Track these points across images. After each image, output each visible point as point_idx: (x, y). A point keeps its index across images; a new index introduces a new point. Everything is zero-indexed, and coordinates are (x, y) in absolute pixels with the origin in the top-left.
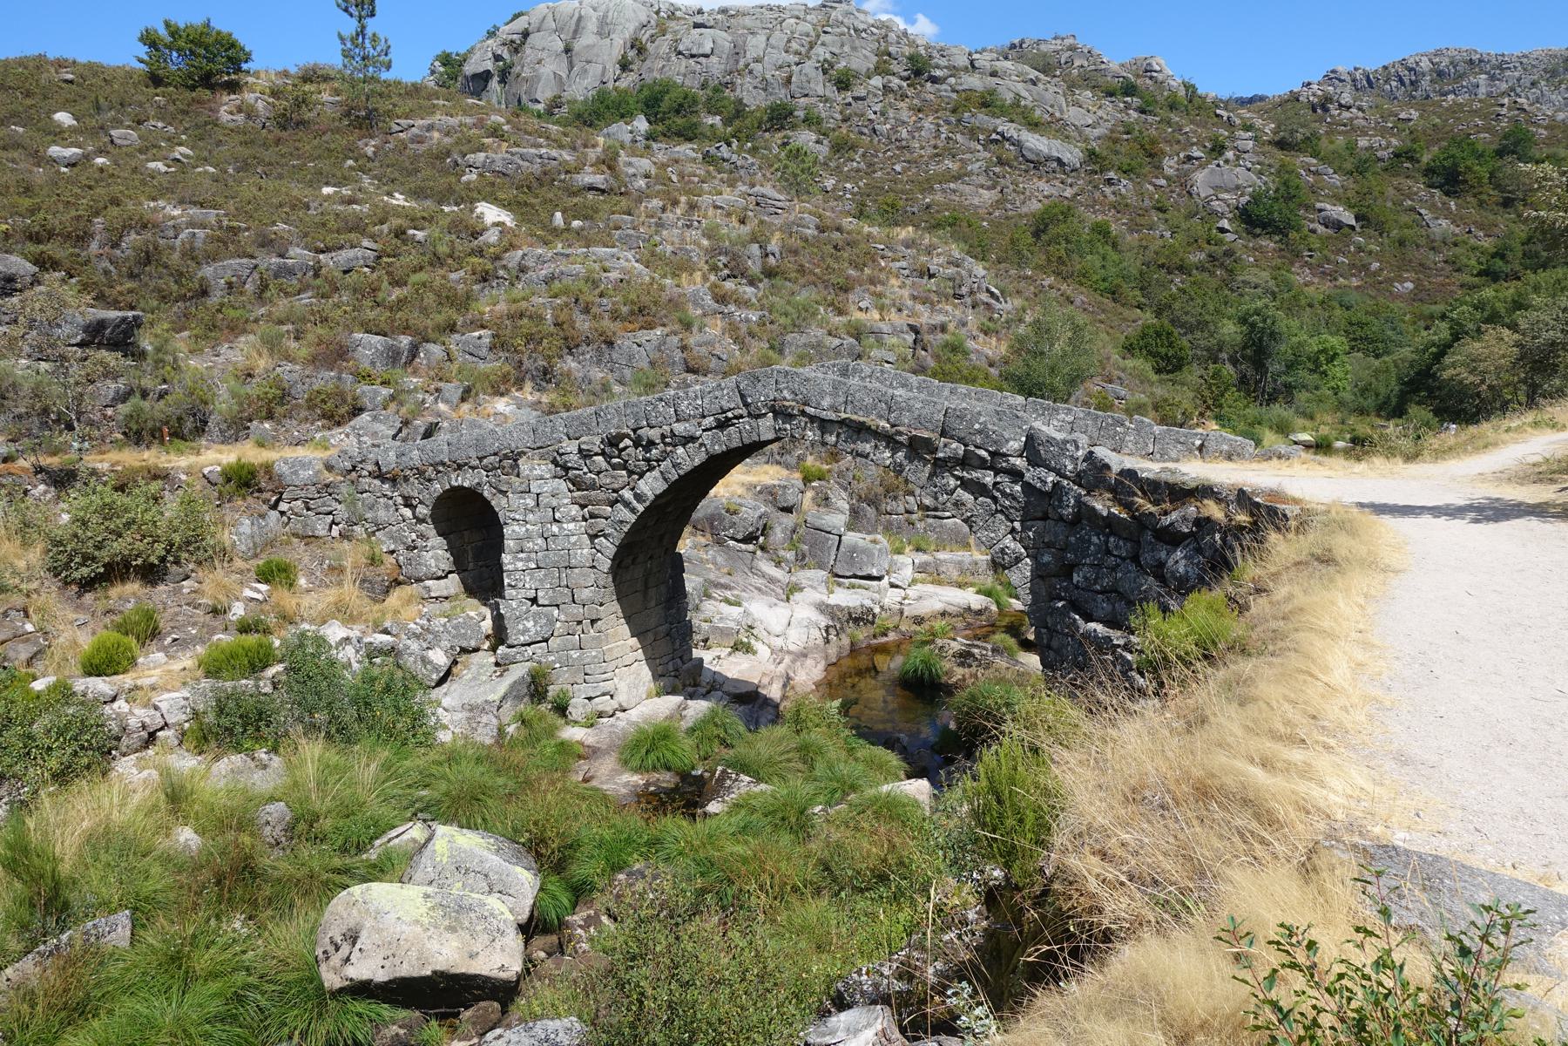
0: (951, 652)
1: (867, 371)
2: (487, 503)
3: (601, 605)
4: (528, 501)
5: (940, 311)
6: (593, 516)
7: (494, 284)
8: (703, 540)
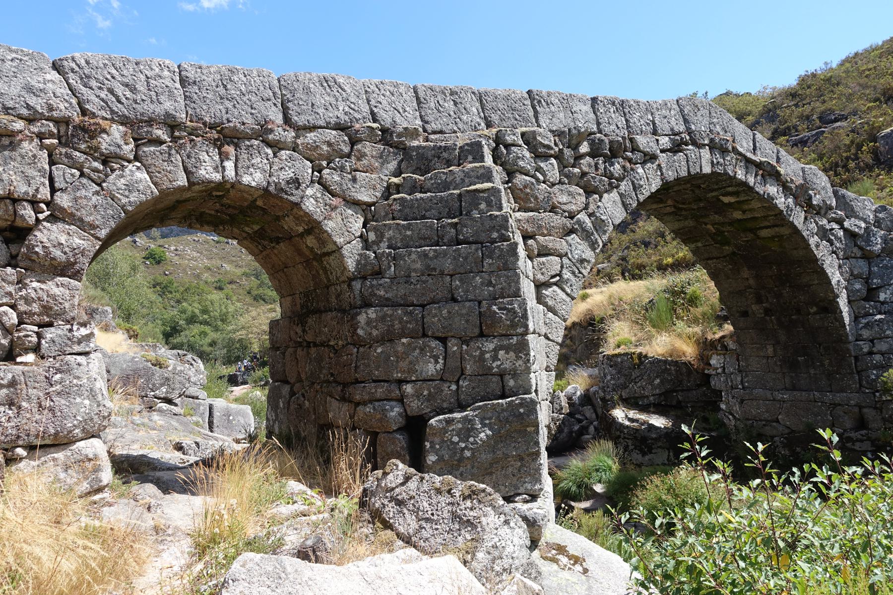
2: (314, 227)
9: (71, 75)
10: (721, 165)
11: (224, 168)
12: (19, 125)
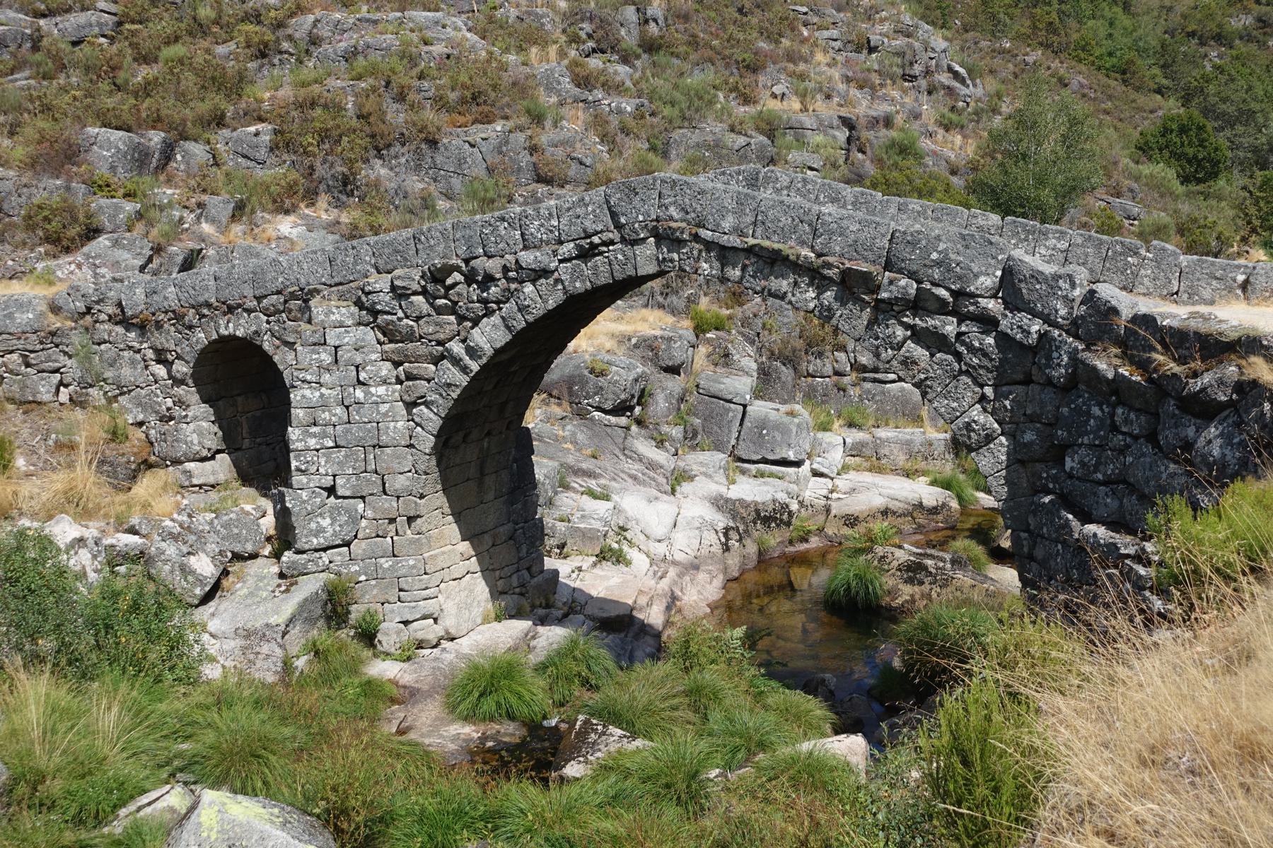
0: (895, 564)
1: (784, 180)
2: (267, 359)
3: (422, 497)
4: (324, 356)
5: (884, 98)
6: (410, 377)
7: (276, 61)
8: (557, 410)
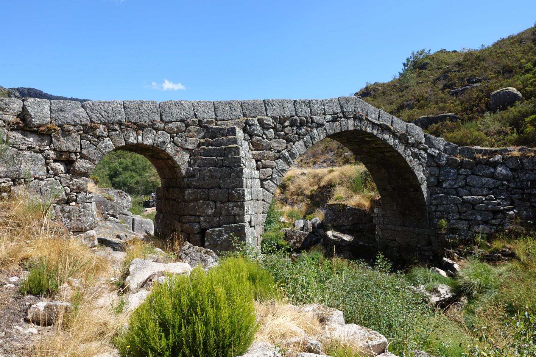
2: (170, 158)
9: (87, 109)
10: (359, 126)
11: (138, 139)
12: (71, 128)
